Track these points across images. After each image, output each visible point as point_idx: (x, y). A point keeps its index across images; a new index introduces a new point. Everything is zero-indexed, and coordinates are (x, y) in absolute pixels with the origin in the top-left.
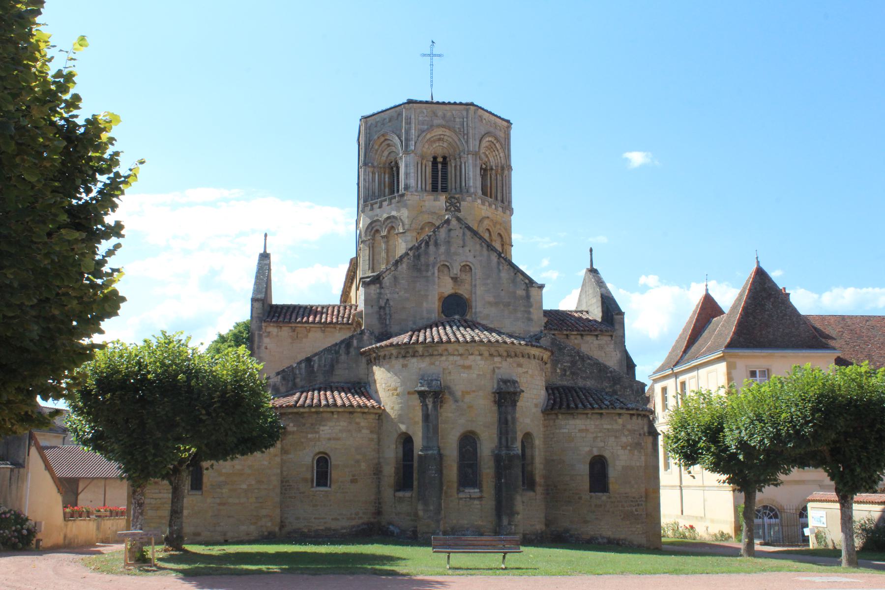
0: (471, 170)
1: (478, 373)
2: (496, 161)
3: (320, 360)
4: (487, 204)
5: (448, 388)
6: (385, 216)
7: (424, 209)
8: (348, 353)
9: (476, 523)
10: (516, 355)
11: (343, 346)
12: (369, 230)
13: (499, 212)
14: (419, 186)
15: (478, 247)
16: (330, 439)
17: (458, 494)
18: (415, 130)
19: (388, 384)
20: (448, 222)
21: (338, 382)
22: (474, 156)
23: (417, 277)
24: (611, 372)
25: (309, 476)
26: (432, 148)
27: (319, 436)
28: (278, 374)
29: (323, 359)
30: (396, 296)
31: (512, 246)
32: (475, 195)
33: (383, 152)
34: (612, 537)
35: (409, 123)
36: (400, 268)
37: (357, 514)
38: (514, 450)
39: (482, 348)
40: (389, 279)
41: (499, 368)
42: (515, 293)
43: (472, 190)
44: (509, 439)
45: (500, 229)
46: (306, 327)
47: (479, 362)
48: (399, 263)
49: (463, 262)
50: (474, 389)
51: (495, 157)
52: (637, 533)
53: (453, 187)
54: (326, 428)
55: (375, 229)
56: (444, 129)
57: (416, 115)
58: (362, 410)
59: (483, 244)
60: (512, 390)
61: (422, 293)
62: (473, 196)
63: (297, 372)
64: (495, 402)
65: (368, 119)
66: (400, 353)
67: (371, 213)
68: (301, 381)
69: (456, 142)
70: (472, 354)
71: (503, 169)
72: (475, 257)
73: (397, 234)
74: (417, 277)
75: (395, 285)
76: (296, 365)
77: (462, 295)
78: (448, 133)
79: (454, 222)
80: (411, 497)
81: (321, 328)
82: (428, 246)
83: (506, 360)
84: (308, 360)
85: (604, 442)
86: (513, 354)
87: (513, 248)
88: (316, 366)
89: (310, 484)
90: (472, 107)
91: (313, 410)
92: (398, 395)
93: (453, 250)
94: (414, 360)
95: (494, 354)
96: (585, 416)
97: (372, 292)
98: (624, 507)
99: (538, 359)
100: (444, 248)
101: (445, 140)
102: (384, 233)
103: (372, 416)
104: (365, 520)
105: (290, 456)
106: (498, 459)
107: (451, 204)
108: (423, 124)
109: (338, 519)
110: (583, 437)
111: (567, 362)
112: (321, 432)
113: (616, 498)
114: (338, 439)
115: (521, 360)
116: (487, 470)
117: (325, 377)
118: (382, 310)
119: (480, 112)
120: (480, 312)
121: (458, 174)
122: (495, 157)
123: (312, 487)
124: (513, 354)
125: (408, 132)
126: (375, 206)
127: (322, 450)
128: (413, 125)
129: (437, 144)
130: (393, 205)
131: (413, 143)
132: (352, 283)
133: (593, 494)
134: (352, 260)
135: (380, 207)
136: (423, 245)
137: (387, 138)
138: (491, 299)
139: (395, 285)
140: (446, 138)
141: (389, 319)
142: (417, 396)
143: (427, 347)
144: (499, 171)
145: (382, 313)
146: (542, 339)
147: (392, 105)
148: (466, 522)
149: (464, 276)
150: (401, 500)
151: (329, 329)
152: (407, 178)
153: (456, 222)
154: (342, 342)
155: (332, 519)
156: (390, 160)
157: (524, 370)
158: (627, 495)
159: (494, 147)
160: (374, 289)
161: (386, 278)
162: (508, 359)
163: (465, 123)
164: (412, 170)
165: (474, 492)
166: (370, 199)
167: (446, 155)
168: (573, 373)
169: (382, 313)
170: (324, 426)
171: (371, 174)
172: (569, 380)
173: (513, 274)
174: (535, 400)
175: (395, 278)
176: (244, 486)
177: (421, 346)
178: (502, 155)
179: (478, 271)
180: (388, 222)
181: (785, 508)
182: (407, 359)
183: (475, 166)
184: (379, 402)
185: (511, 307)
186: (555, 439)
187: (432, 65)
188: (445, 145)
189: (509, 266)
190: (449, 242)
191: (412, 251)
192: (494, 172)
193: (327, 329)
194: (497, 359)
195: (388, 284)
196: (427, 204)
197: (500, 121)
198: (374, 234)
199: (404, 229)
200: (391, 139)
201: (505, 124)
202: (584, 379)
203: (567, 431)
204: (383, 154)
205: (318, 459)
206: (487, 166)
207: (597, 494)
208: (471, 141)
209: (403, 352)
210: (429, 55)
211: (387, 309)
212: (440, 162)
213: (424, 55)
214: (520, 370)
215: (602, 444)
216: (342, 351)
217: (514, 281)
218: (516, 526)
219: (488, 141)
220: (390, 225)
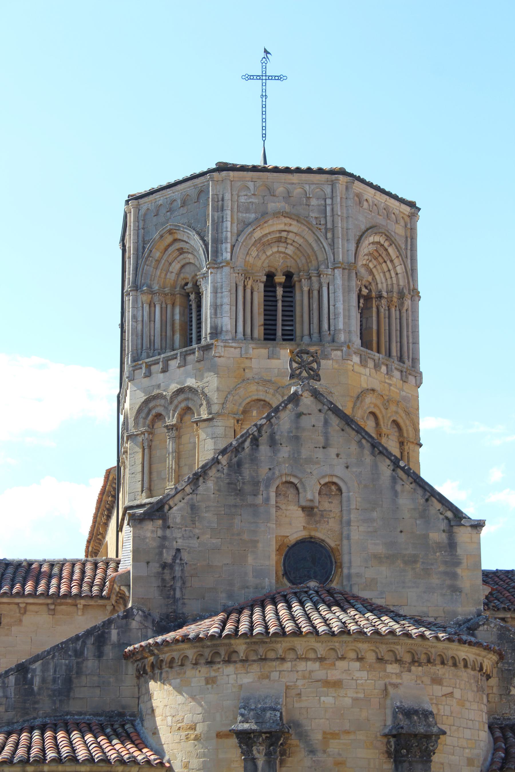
0: (341, 298)
1: (355, 695)
2: (389, 282)
3: (45, 668)
4: (371, 364)
5: (297, 725)
6: (174, 387)
7: (249, 374)
8: (100, 655)
10: (429, 661)
11: (92, 640)
12: (143, 415)
14: (240, 329)
15: (354, 447)
18: (232, 223)
19: (178, 718)
20: (295, 398)
21: (80, 714)
22: (346, 271)
23: (235, 506)
26: (264, 257)
29: (51, 666)
30: (194, 543)
31: (421, 445)
32: (348, 347)
33: (170, 264)
35: (220, 208)
36: (201, 489)
39: (363, 646)
40: (180, 510)
41: (396, 686)
42: (426, 537)
43: (342, 337)
45: (396, 413)
46: (18, 604)
47: (357, 674)
48: (201, 479)
49: (324, 477)
50: (347, 726)
51: (387, 274)
53: (306, 332)
55: (154, 412)
56: (287, 220)
59: (364, 441)
60: (421, 729)
61: (245, 537)
62: (344, 349)
64: (388, 753)
65: (141, 201)
66: (201, 655)
67: (146, 382)
68: (6, 711)
69: (310, 245)
70: (343, 658)
71: (401, 296)
72: (347, 467)
73: (197, 423)
74: (235, 506)
77: (323, 541)
78: (295, 227)
79: (307, 400)
81: (48, 604)
82: (258, 446)
83: (410, 671)
86: (423, 658)
87: (421, 450)
88: (37, 681)
90: (341, 177)
92: (196, 739)
93: (305, 453)
94: (230, 669)
95: (386, 658)
97: (149, 534)
99: (474, 669)
100: (288, 449)
101: (289, 241)
102: (172, 421)
107: (302, 365)
108: (247, 210)
115: (439, 670)
117: (54, 703)
119: (358, 186)
120: (358, 575)
121: (315, 306)
122: (387, 274)
124: (423, 658)
125: (218, 225)
126: (155, 368)
128: (229, 212)
129: (275, 249)
130: (189, 367)
131: (229, 246)
132: (109, 517)
134: (109, 472)
135: (165, 370)
136: (247, 444)
137: (179, 237)
138: (380, 549)
139: (193, 522)
140: (291, 236)
141: (181, 589)
142: (234, 741)
143: (255, 643)
144: (395, 300)
145: (167, 577)
146: (481, 628)
147: (188, 175)
149: (326, 505)
151: (63, 607)
152: (216, 314)
153: (312, 399)
154: (89, 633)
156: (184, 279)
157: (447, 690)
159: (384, 254)
161: (175, 508)
162: (413, 668)
163: (329, 209)
164: (226, 299)
166: (144, 355)
167: (292, 270)
169: (167, 577)
171: (146, 307)
173: (422, 501)
174: (467, 751)
175: (193, 508)
177: (241, 641)
178: (399, 269)
180: (181, 397)
182: (216, 667)
183: (347, 290)
184: (159, 752)
185: (418, 565)
187: (264, 96)
189: (413, 485)
190: (297, 438)
191: (226, 456)
192: (384, 302)
193: (59, 608)
194: (392, 668)
195: (178, 520)
196: (254, 363)
197: (397, 203)
198: (153, 422)
199: (210, 413)
200: (185, 238)
204: (171, 270)
206: (370, 291)
209: (207, 653)
210: (259, 77)
211: (177, 568)
212: (280, 284)
213: (250, 77)
214: (438, 690)
216: (89, 650)
217: (424, 515)
219: (373, 243)
220: (183, 405)
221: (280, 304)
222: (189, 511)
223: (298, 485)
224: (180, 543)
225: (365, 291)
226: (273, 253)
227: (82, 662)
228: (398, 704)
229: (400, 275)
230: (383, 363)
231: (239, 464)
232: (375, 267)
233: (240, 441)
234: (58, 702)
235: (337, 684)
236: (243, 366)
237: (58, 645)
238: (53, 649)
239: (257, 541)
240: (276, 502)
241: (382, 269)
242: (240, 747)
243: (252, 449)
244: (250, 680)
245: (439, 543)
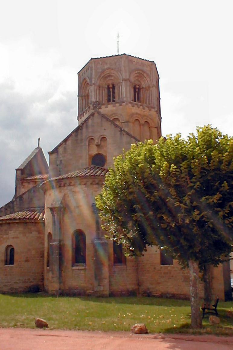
9: (82, 285)
13: (146, 110)
16: (13, 238)
17: (73, 266)
36: (67, 143)
37: (29, 279)
38: (103, 240)
45: (146, 119)
54: (12, 232)
57: (96, 65)
65: (80, 73)
77: (102, 154)
79: (96, 115)
89: (4, 263)
91: (4, 222)
104: (35, 283)
109: (17, 283)
112: (10, 234)
116: (89, 253)
121: (119, 92)
123: (6, 264)
126: (82, 116)
127: (9, 244)
129: (109, 79)
131: (94, 79)
140: (112, 74)
153: (97, 114)
155: (14, 283)
160: (54, 156)
170: (11, 231)
175: (65, 148)
179: (109, 140)
188: (113, 78)
195: (61, 152)
201: (151, 63)
207: (165, 265)
208: (124, 74)
212: (111, 88)
218: (103, 286)
221: (111, 93)
223: (94, 139)
224: (62, 159)
225: (137, 87)
226: (109, 80)
229: (149, 82)
230: (141, 106)
240: (89, 145)
242: (51, 212)
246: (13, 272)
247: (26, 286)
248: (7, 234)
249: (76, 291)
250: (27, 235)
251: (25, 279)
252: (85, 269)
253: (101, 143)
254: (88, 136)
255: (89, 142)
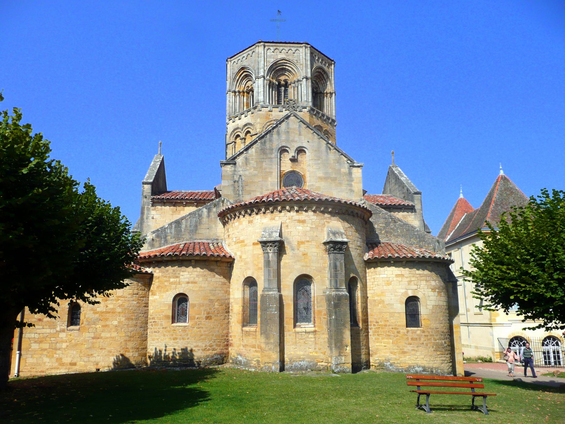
1: (311, 226)
7: (271, 117)
9: (311, 354)
12: (232, 136)
14: (267, 101)
15: (310, 135)
16: (188, 283)
19: (238, 238)
24: (417, 231)
25: (170, 314)
26: (277, 76)
27: (179, 280)
28: (154, 232)
30: (247, 173)
34: (427, 365)
37: (211, 346)
42: (340, 170)
44: (338, 281)
52: (446, 362)
58: (216, 259)
59: (315, 134)
61: (268, 170)
63: (169, 232)
75: (247, 164)
76: (167, 226)
80: (256, 332)
81: (194, 203)
84: (178, 223)
85: (417, 285)
88: (183, 226)
93: (291, 138)
94: (258, 217)
96: (400, 264)
98: (436, 340)
99: (361, 218)
103: (225, 265)
104: (218, 351)
105: (155, 297)
106: (329, 299)
110: (399, 281)
111: (382, 223)
112: (181, 276)
113: (429, 332)
114: (195, 283)
117: (190, 235)
118: (236, 183)
122: (323, 85)
129: (281, 73)
133: (409, 329)
139: (247, 164)
140: (287, 67)
142: (260, 246)
143: (268, 205)
148: (302, 353)
150: (248, 333)
158: (438, 330)
159: (322, 77)
163: (301, 57)
164: (261, 89)
165: (308, 327)
168: (386, 232)
170: (183, 271)
172: (384, 238)
174: (358, 250)
175: (246, 159)
176: (115, 323)
177: (263, 204)
181: (532, 339)
185: (337, 181)
186: (376, 283)
189: (334, 150)
190: (288, 132)
195: (240, 164)
196: (273, 113)
197: (327, 59)
202: (397, 236)
203: (385, 276)
205: (179, 299)
211: (240, 182)
215: (415, 287)
220: (247, 130)
222: (245, 160)
224: (241, 173)
227: (202, 219)
228: (330, 229)
231: (265, 142)
232: (319, 82)
233: (265, 133)
234: (192, 235)
235: (303, 222)
236: (269, 114)
237: (192, 213)
238: (190, 214)
239: (272, 172)
241: (321, 83)
243: (270, 136)
244: (267, 221)
245: (345, 173)
246: (187, 335)
247: (207, 356)
248: (177, 277)
249: (302, 363)
250: (209, 279)
251: (206, 346)
252: (315, 331)
253: (297, 157)
254: (280, 146)
255: (280, 155)
